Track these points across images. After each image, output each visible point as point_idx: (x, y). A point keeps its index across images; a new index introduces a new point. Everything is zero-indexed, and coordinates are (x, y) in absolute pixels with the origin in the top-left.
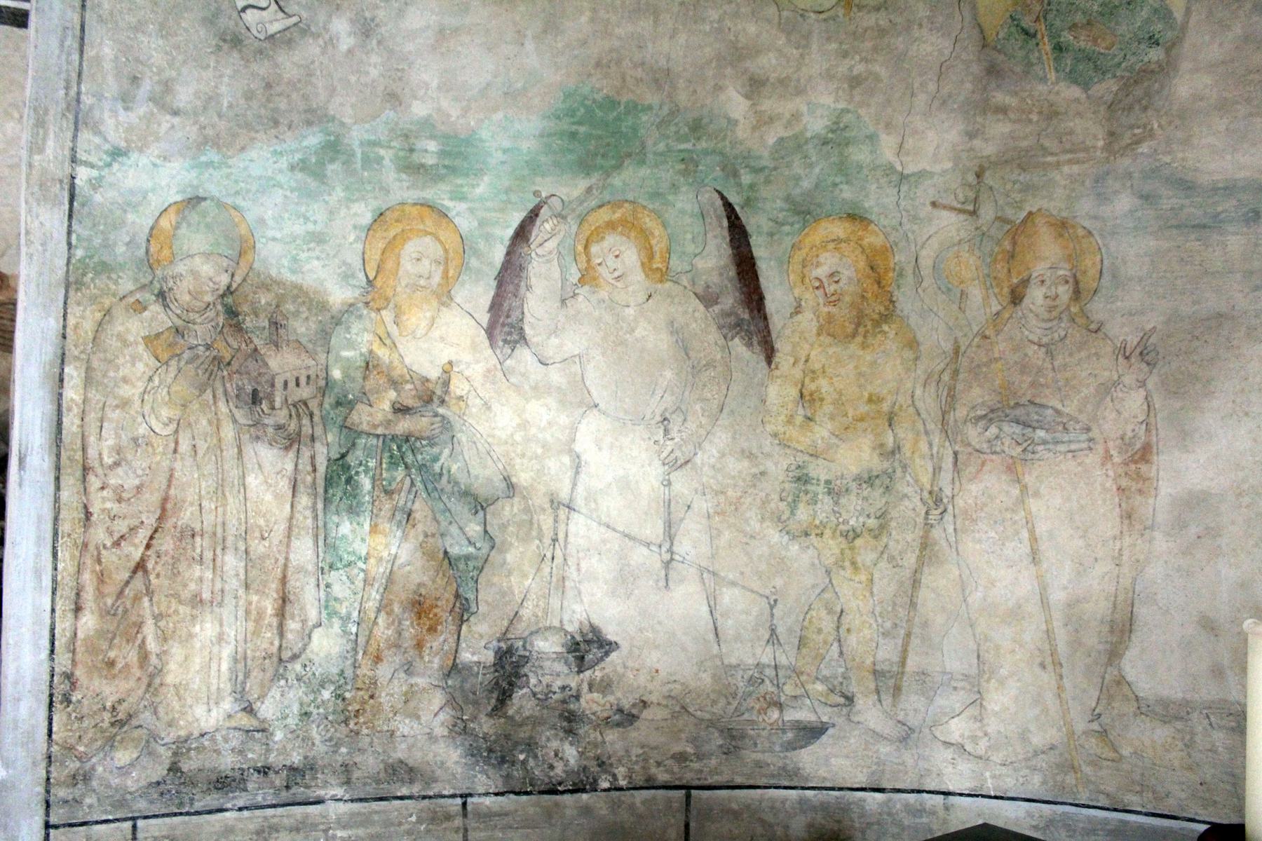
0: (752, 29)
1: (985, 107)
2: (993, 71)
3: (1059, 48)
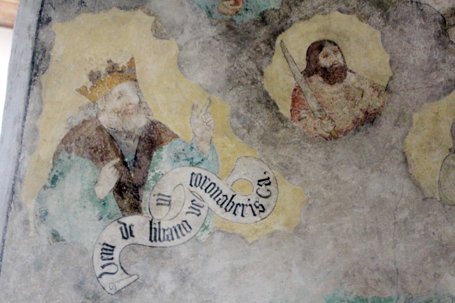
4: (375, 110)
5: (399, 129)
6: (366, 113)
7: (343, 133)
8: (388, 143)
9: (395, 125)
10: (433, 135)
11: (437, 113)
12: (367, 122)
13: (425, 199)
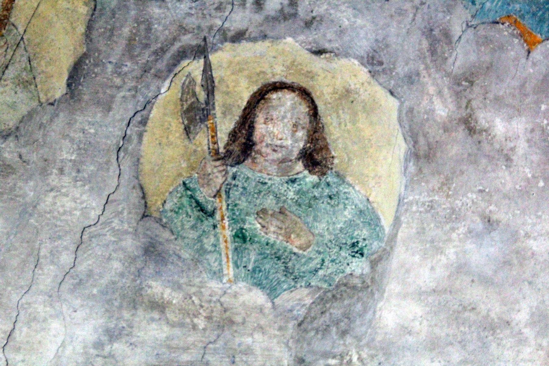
1: (136, 299)
2: (152, 251)
3: (241, 237)
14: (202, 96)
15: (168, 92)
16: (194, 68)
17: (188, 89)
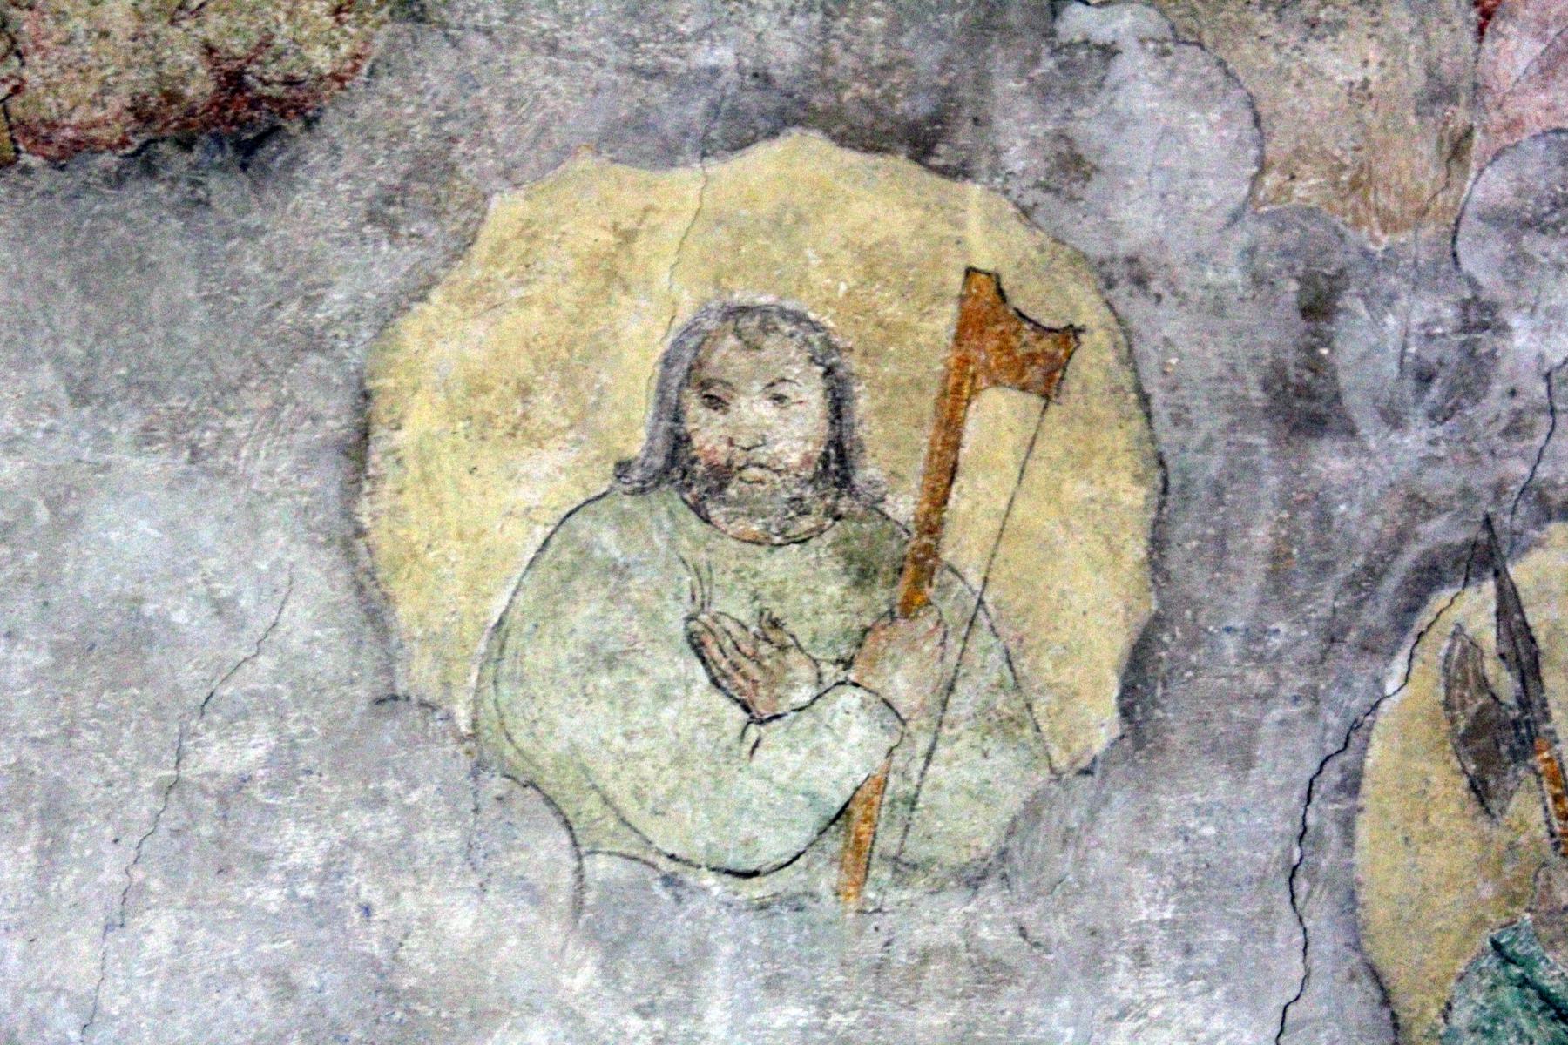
0: (462, 919)
4: (290, 82)
5: (385, 248)
6: (233, 81)
7: (52, 151)
8: (293, 307)
9: (372, 218)
10: (564, 354)
11: (628, 237)
12: (218, 139)
13: (386, 701)
14: (1506, 684)
15: (1408, 689)
16: (1471, 608)
17: (1462, 670)
